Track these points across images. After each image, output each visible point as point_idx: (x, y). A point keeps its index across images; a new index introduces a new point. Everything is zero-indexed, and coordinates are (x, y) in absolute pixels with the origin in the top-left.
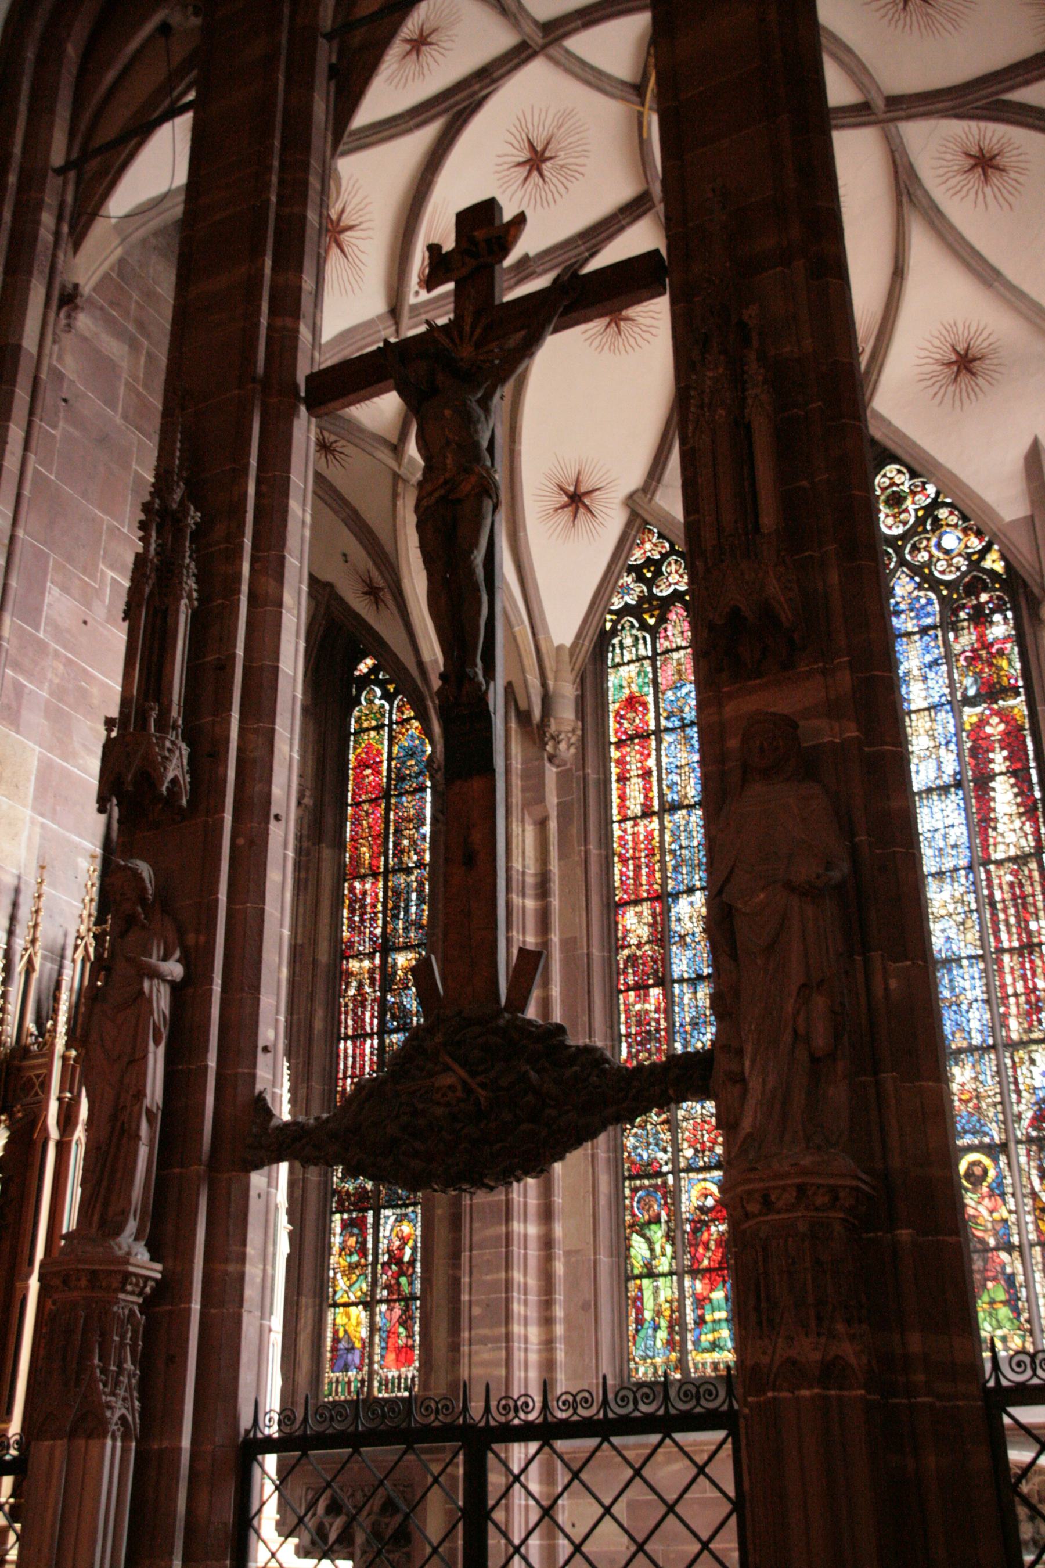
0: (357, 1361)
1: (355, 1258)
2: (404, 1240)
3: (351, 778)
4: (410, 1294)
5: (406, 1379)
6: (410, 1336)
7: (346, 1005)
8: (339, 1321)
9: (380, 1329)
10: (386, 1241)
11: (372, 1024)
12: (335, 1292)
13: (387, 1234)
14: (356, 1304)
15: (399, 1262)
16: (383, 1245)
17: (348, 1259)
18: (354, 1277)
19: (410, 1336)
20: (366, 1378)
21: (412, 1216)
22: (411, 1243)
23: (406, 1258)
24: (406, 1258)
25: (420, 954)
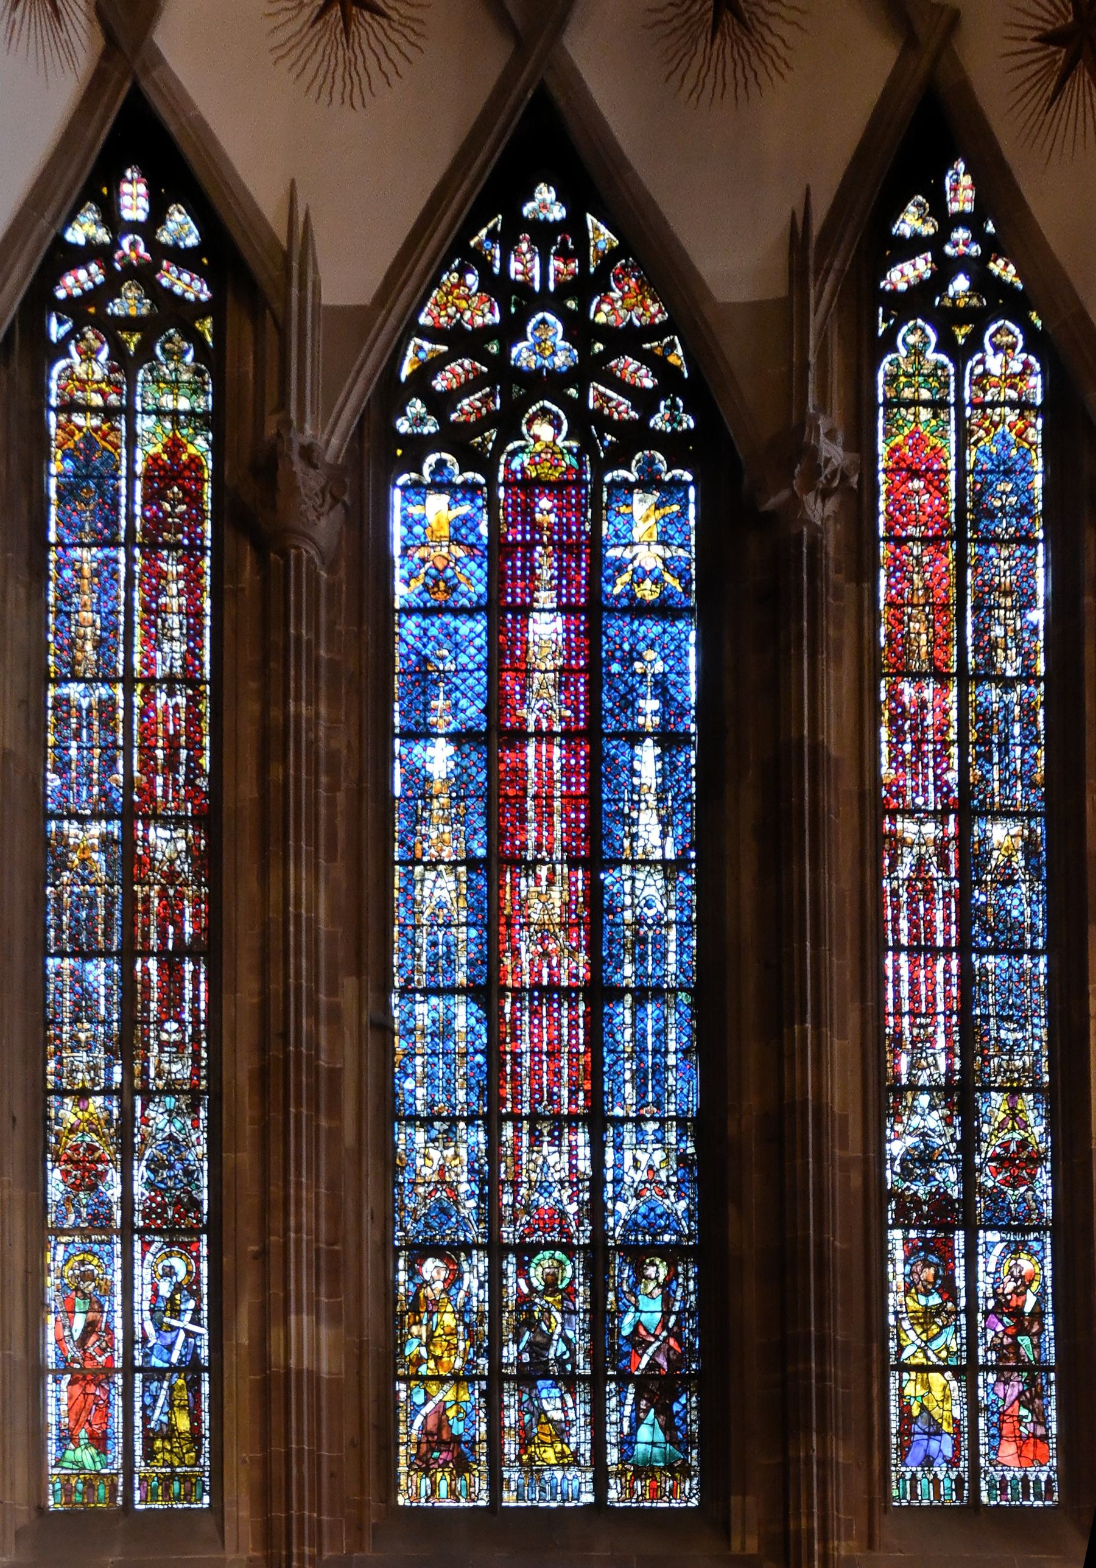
0: (948, 1452)
1: (935, 1300)
2: (1024, 1283)
3: (883, 488)
4: (1037, 1360)
5: (1037, 1481)
6: (1041, 1419)
7: (895, 893)
8: (909, 1390)
9: (987, 1407)
10: (990, 1280)
11: (947, 932)
12: (901, 1349)
13: (991, 1268)
14: (941, 1370)
15: (1017, 1313)
16: (984, 1285)
17: (922, 1300)
18: (935, 1329)
19: (1041, 1419)
20: (966, 1477)
21: (1036, 1246)
22: (1035, 1285)
23: (1028, 1309)
24: (1028, 1309)
25: (1032, 831)
